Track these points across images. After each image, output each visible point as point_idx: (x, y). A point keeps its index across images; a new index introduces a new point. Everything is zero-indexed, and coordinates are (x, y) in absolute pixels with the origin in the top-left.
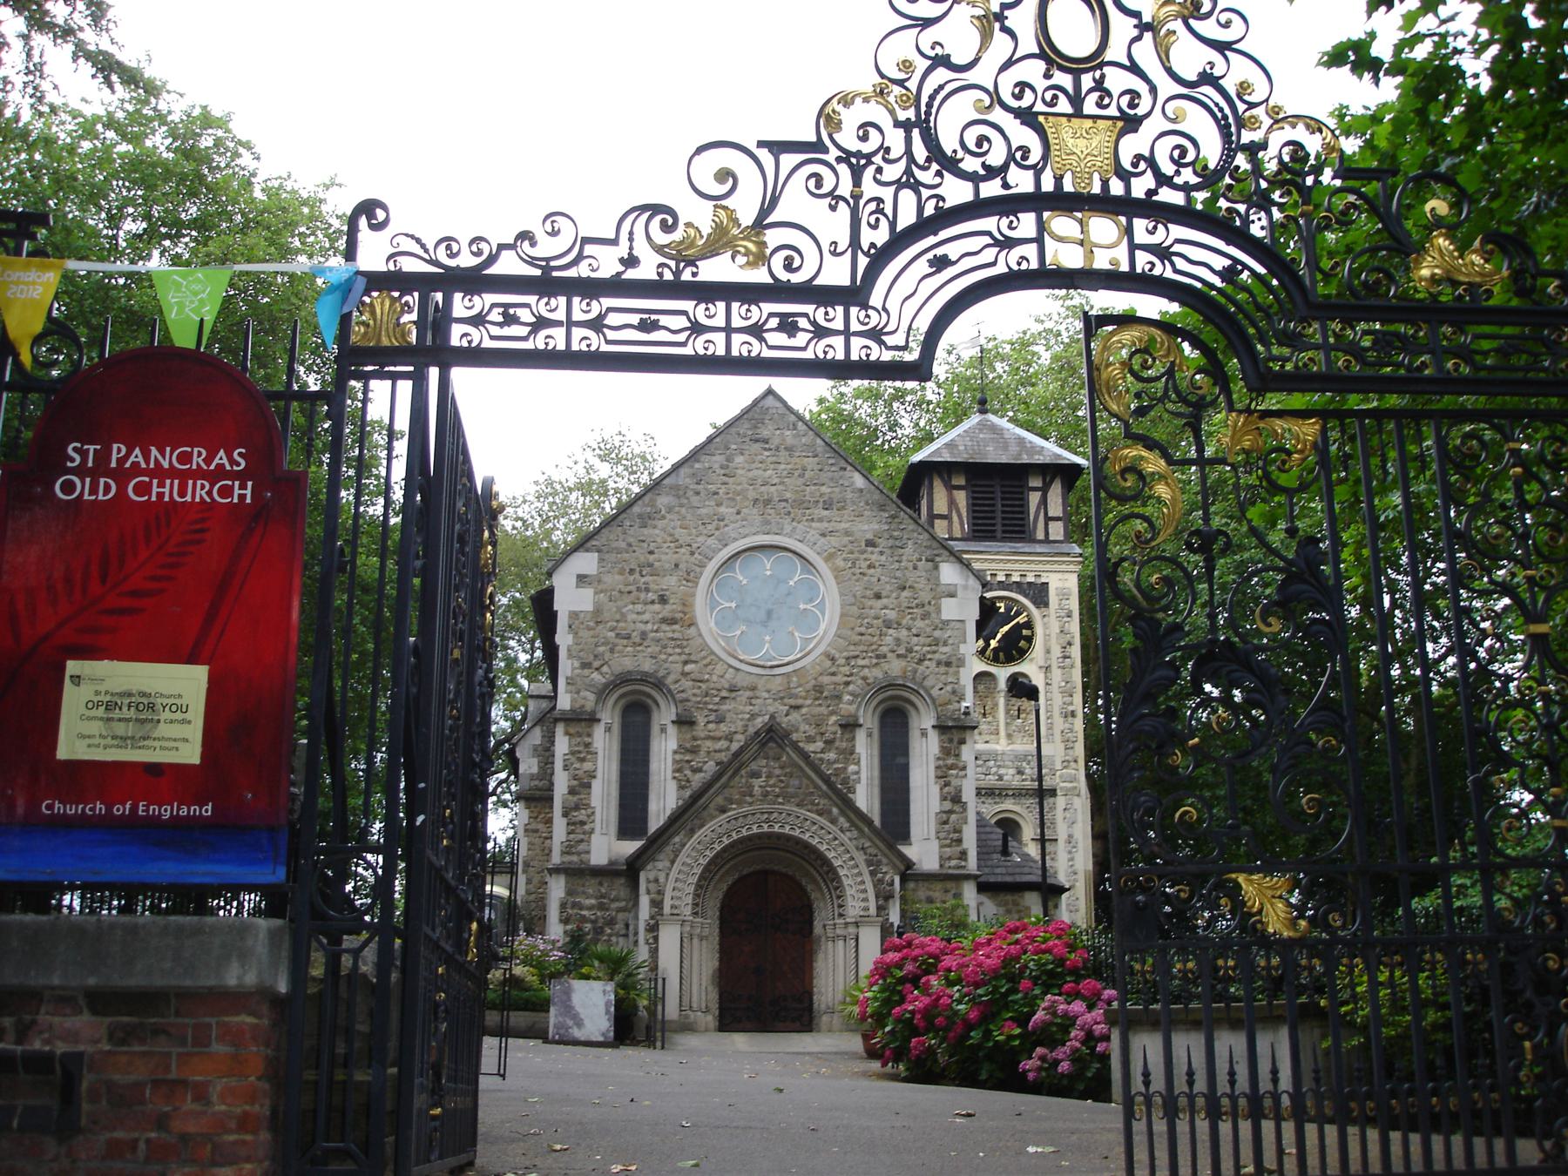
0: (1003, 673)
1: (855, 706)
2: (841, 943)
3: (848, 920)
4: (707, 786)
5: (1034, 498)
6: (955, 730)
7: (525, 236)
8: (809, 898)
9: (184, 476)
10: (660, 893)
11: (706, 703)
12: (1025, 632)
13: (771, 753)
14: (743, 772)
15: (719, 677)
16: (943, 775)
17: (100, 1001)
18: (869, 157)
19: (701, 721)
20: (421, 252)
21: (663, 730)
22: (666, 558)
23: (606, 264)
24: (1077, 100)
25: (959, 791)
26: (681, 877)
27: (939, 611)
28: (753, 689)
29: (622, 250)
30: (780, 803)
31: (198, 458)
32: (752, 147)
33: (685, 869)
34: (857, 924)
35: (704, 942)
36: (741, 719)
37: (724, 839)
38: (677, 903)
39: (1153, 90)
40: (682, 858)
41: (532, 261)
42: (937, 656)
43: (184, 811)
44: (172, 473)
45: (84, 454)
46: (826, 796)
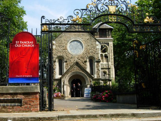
0: (104, 54)
4: (69, 69)
5: (107, 32)
6: (98, 62)
7: (58, 19)
9: (27, 44)
10: (64, 82)
12: (106, 49)
14: (74, 67)
15: (70, 56)
16: (97, 67)
17: (24, 94)
18: (91, 10)
19: (68, 61)
20: (48, 21)
22: (63, 42)
23: (66, 22)
24: (111, 4)
25: (99, 69)
27: (96, 47)
28: (74, 57)
29: (68, 20)
31: (28, 42)
32: (80, 9)
36: (73, 61)
39: (119, 3)
40: (67, 77)
41: (59, 22)
42: (96, 53)
43: (29, 76)
44: (26, 44)
45: (17, 42)
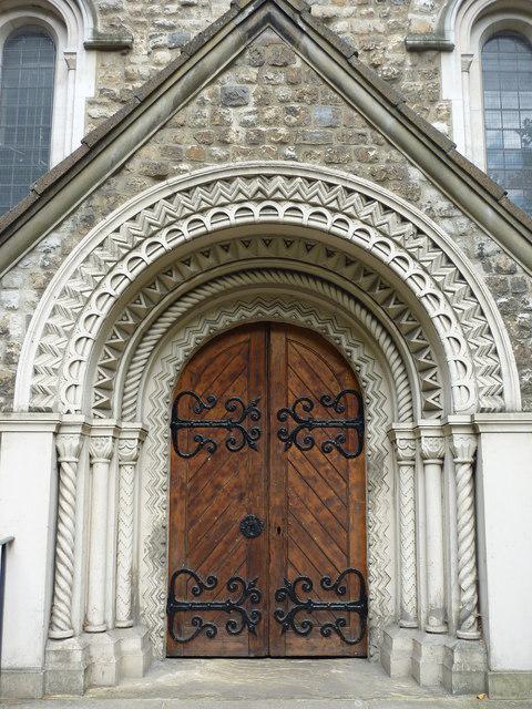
1: (436, 17)
2: (433, 471)
3: (452, 419)
8: (355, 376)
11: (152, 14)
13: (268, 53)
14: (205, 94)
19: (141, 45)
21: (70, 66)
26: (58, 321)
30: (287, 158)
33: (67, 304)
34: (474, 430)
35: (127, 472)
37: (162, 238)
38: (46, 381)
40: (61, 278)
46: (393, 141)
